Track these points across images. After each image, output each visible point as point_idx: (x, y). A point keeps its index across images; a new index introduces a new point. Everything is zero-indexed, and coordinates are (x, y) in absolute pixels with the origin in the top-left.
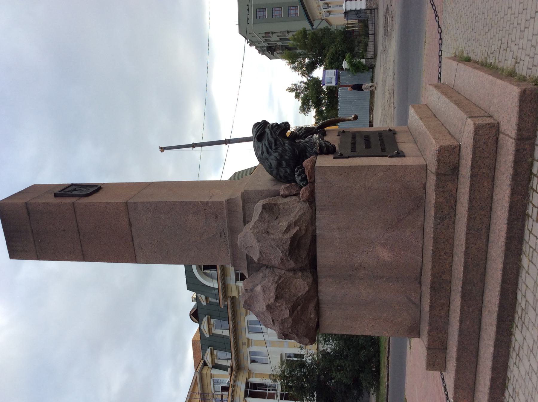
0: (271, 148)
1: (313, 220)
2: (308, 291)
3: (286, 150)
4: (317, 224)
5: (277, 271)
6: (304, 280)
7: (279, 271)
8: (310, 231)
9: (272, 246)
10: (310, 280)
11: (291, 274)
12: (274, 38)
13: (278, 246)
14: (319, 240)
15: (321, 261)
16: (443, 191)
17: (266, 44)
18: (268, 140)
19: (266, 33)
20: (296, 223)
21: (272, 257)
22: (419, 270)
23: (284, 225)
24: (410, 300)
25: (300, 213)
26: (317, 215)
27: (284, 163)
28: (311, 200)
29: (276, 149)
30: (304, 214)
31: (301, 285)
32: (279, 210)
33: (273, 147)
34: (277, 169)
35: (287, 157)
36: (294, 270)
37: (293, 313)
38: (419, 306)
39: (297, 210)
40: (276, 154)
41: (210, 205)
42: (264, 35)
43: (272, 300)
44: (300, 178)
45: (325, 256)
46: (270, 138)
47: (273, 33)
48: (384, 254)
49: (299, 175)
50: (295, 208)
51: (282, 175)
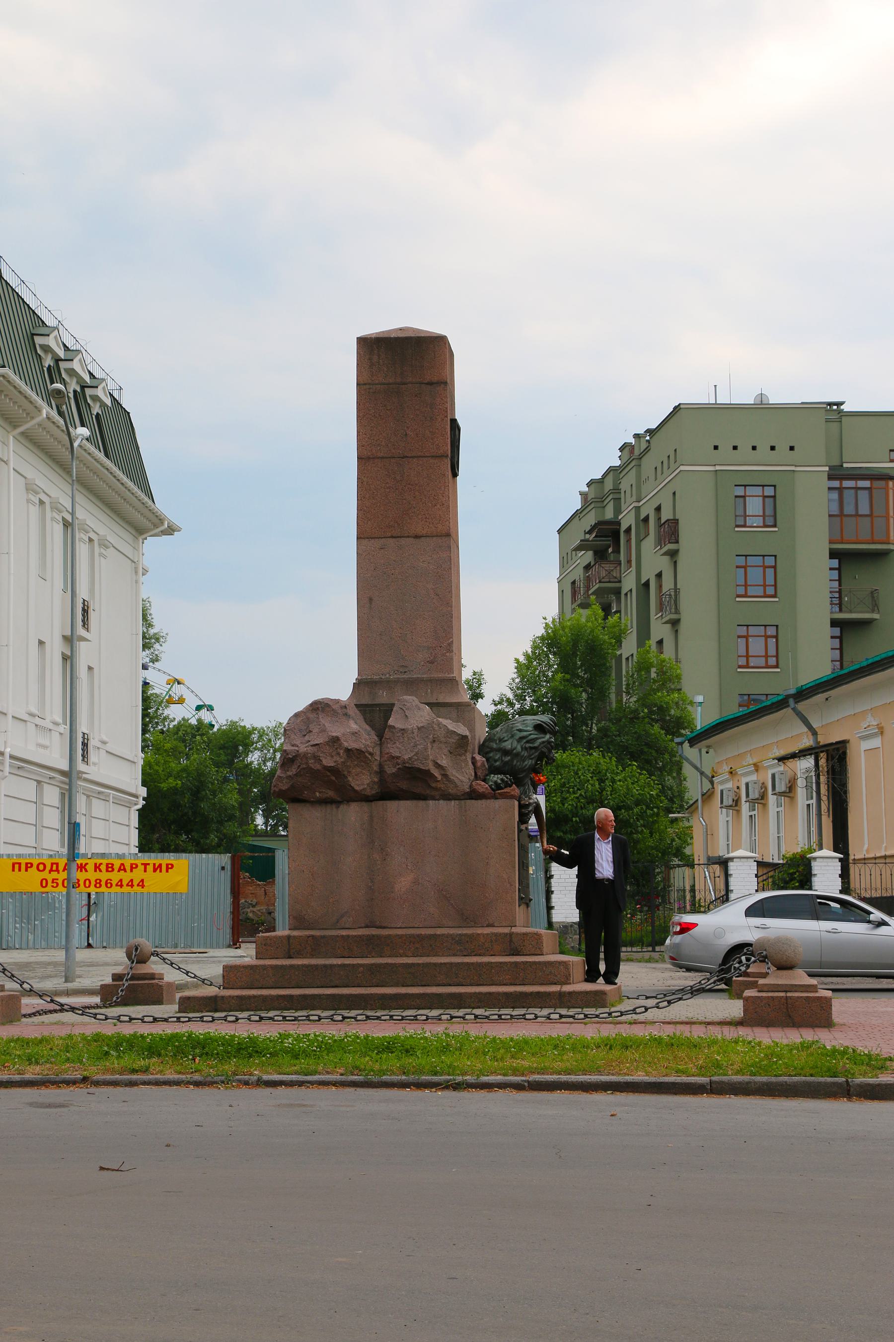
0: (528, 742)
1: (447, 797)
2: (356, 791)
3: (524, 761)
4: (441, 802)
5: (377, 751)
6: (368, 785)
7: (378, 753)
8: (433, 793)
9: (416, 746)
10: (369, 792)
11: (376, 768)
12: (651, 558)
13: (417, 754)
14: (421, 803)
15: (392, 805)
16: (492, 941)
17: (627, 520)
18: (537, 739)
19: (674, 523)
20: (445, 776)
21: (397, 744)
22: (386, 925)
23: (444, 762)
24: (342, 916)
25: (456, 781)
26: (453, 802)
27: (508, 758)
28: (473, 795)
29: (526, 749)
30: (456, 786)
31: (362, 780)
32: (460, 755)
33: (528, 745)
34: (499, 750)
35: (515, 762)
36: (381, 771)
37: (329, 771)
38: (334, 927)
39: (460, 777)
40: (519, 748)
41: (448, 654)
42: (666, 515)
43: (346, 744)
44: (499, 781)
45: (399, 812)
46: (540, 741)
47: (673, 554)
48: (403, 883)
49: (502, 780)
50: (462, 776)
51: (491, 755)
